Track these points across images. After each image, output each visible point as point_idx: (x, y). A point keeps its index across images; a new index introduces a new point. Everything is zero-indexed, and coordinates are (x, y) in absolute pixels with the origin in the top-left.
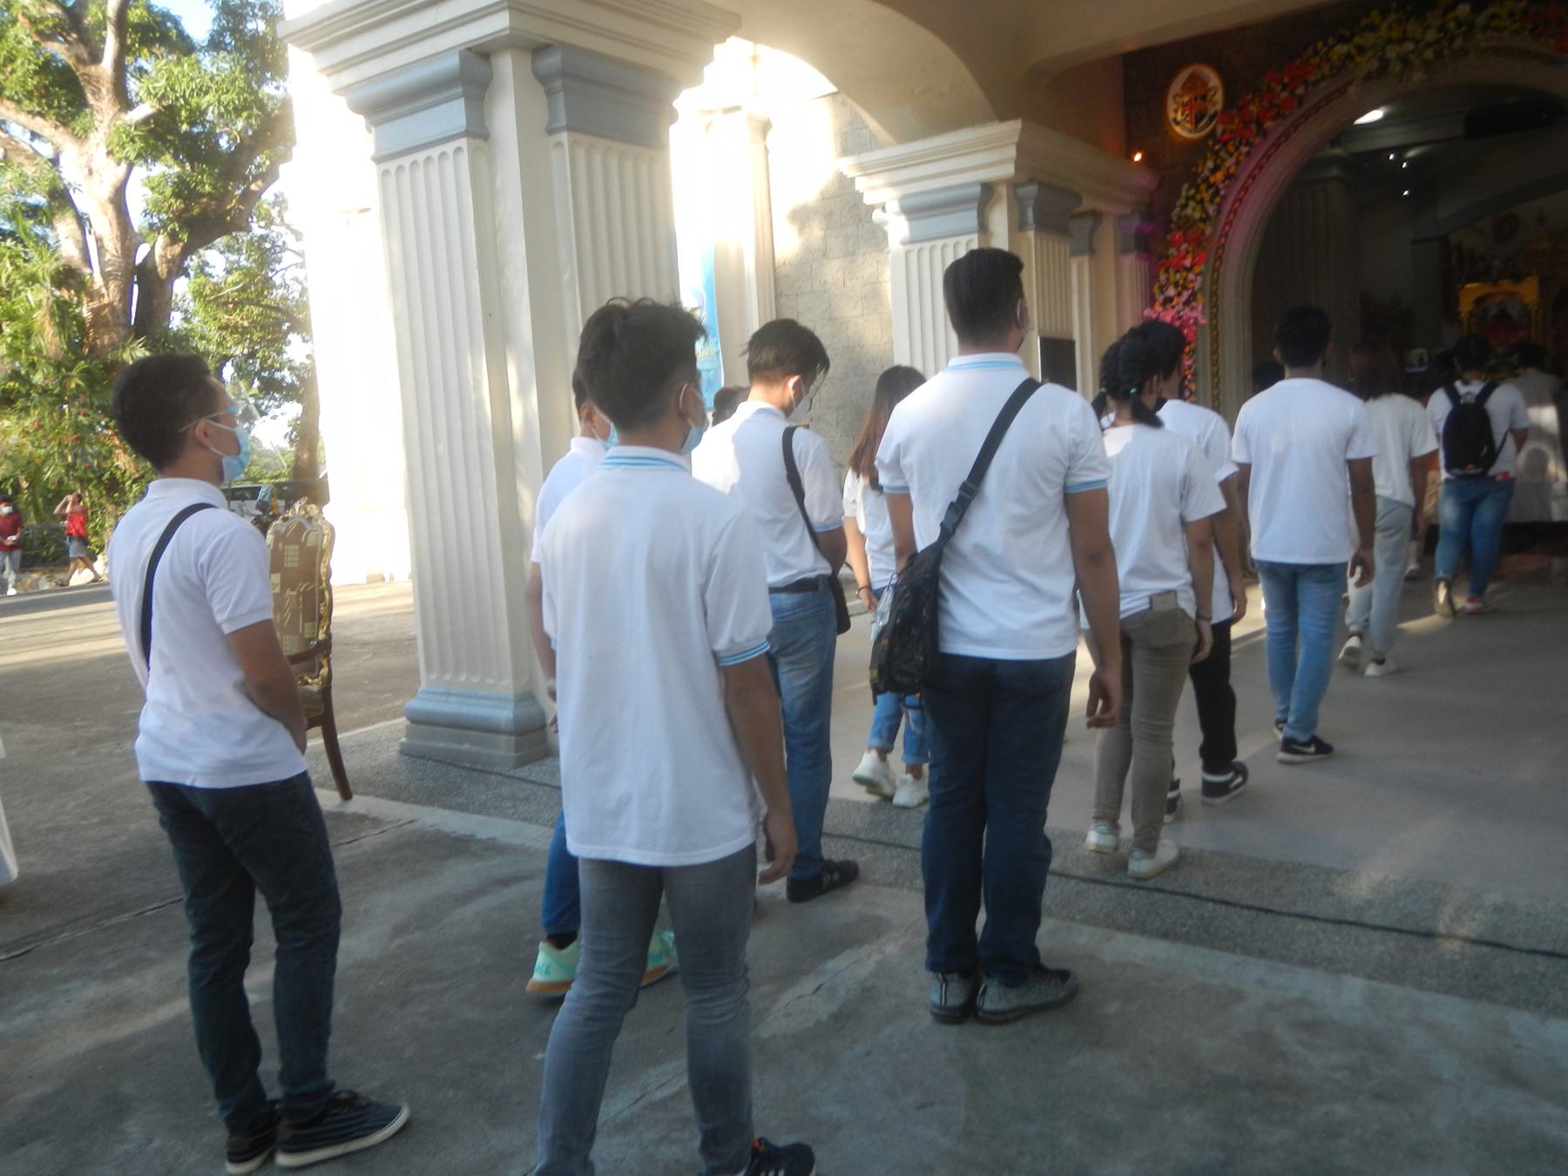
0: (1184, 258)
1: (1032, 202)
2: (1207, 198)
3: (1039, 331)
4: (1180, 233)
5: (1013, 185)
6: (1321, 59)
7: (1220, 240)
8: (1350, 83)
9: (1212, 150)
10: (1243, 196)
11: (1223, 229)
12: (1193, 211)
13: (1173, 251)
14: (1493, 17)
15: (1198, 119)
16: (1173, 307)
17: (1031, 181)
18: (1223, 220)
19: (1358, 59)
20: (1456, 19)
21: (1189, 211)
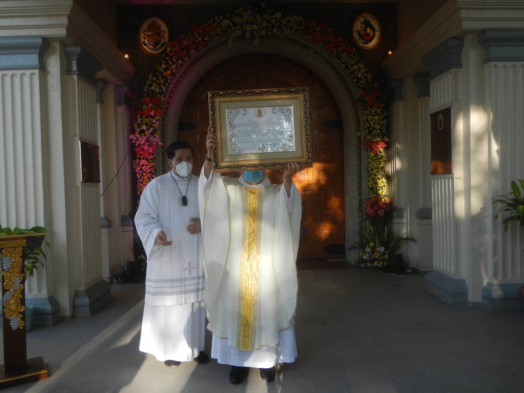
0: (151, 111)
1: (76, 57)
2: (162, 83)
3: (80, 138)
4: (149, 98)
5: (64, 43)
6: (217, 26)
8: (229, 40)
11: (167, 101)
13: (144, 107)
15: (156, 44)
16: (145, 135)
17: (75, 44)
18: (168, 96)
19: (233, 28)
20: (276, 18)
21: (153, 88)
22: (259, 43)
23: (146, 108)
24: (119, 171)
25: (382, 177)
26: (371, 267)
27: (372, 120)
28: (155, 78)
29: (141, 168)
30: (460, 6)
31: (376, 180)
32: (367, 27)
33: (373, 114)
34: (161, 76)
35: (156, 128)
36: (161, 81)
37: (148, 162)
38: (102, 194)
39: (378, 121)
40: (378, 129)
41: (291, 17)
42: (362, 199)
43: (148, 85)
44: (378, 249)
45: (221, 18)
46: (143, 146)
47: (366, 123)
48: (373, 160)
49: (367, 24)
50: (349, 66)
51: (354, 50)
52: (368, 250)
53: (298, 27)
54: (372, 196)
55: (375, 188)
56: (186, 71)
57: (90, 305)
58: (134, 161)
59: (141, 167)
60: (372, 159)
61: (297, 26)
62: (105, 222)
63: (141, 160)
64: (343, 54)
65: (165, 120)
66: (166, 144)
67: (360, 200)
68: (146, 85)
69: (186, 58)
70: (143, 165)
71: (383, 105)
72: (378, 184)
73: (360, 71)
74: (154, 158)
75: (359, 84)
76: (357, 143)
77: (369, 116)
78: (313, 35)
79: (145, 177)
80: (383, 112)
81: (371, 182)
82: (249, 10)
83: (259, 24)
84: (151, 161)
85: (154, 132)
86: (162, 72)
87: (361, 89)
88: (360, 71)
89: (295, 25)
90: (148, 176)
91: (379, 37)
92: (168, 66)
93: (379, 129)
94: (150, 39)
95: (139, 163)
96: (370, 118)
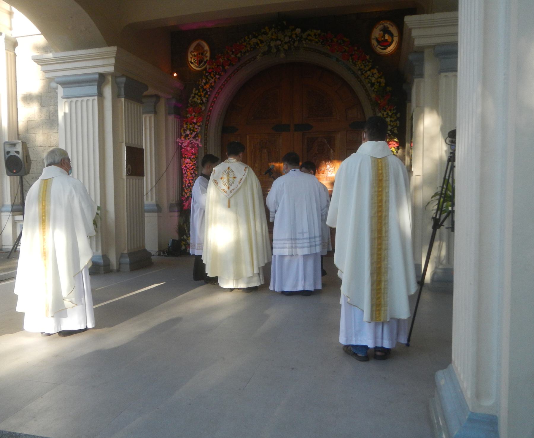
2: (203, 95)
4: (192, 108)
6: (247, 44)
7: (208, 113)
8: (257, 55)
9: (205, 75)
10: (217, 96)
11: (210, 109)
12: (197, 100)
13: (189, 115)
14: (309, 35)
15: (200, 62)
16: (189, 139)
18: (209, 105)
19: (260, 45)
20: (296, 34)
21: (195, 99)
28: (197, 92)
29: (186, 165)
35: (198, 132)
36: (202, 93)
37: (191, 160)
39: (390, 122)
41: (310, 32)
43: (192, 97)
45: (250, 37)
46: (187, 147)
51: (368, 57)
58: (182, 160)
59: (185, 164)
61: (316, 38)
62: (156, 208)
65: (207, 125)
69: (223, 72)
70: (187, 163)
71: (395, 108)
74: (196, 157)
75: (373, 88)
78: (331, 46)
82: (273, 29)
84: (193, 160)
85: (196, 136)
86: (203, 86)
91: (397, 43)
92: (207, 80)
94: (196, 58)
95: (184, 161)
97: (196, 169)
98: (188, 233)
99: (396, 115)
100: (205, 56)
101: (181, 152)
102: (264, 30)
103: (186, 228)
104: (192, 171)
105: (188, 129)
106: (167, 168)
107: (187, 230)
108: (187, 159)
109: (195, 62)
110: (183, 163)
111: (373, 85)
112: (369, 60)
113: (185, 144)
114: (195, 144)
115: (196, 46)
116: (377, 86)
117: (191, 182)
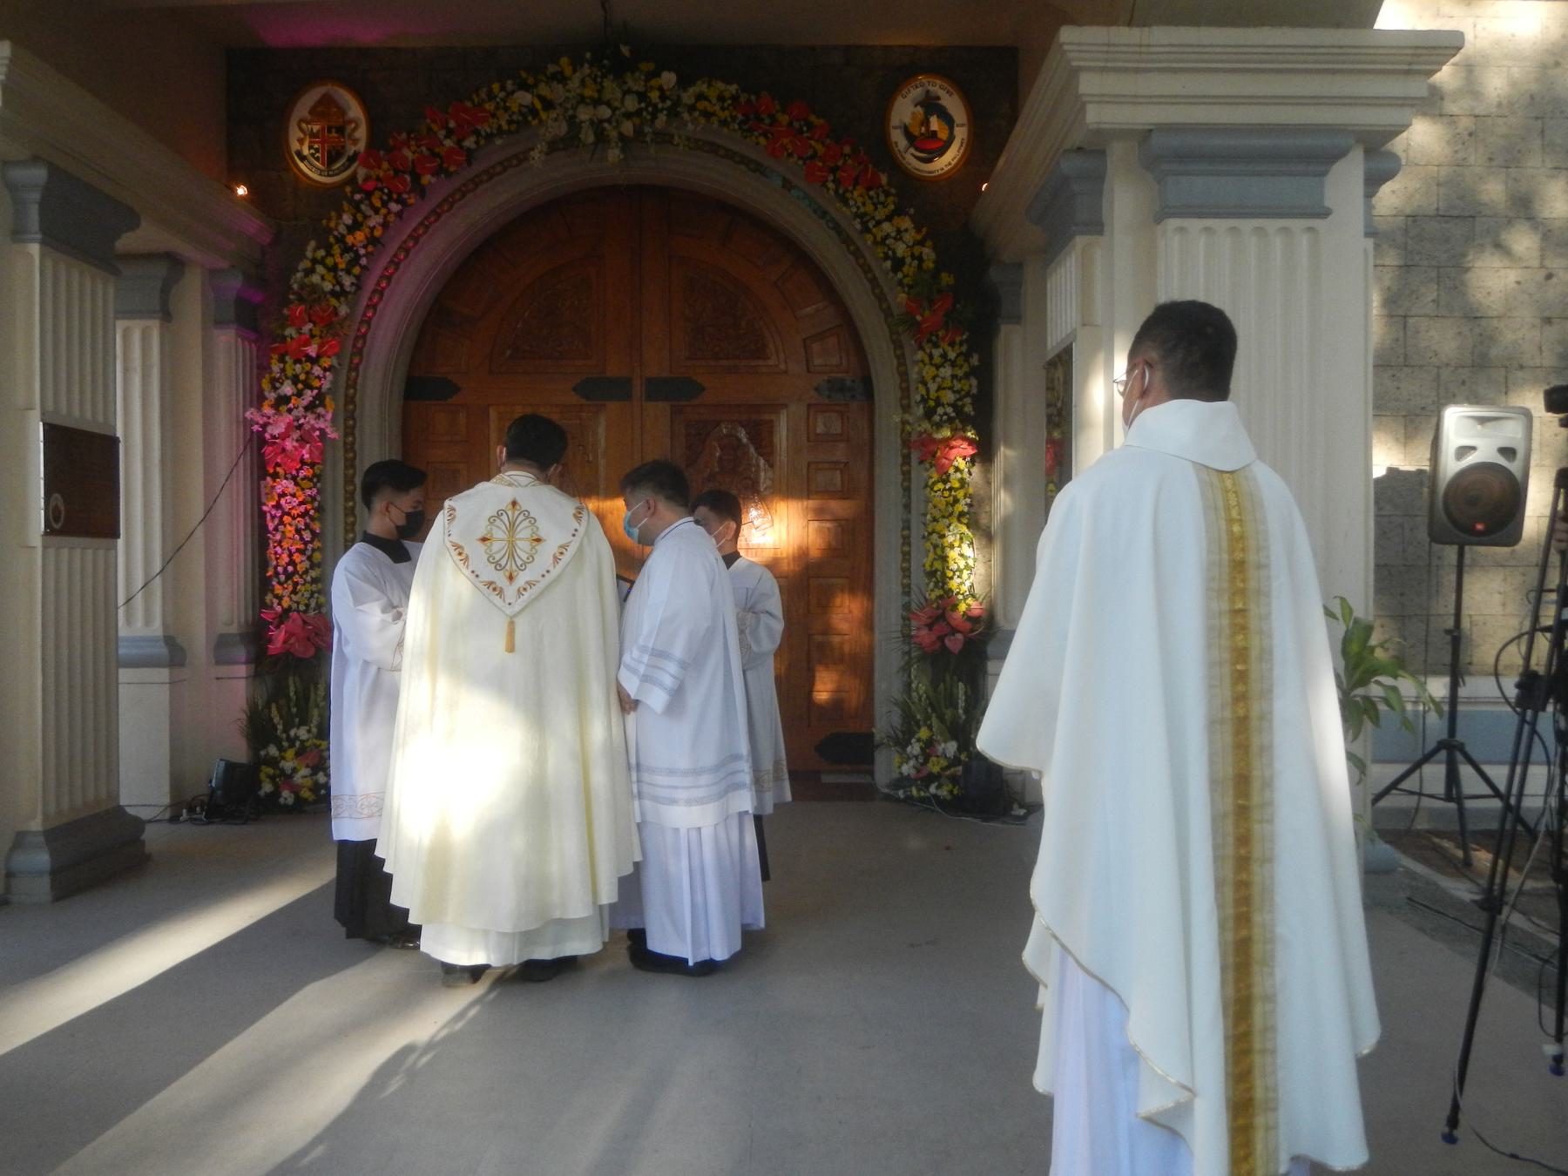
0: (307, 343)
1: (36, 196)
2: (342, 266)
3: (43, 413)
4: (303, 306)
6: (497, 108)
7: (359, 330)
12: (321, 279)
13: (290, 331)
15: (332, 158)
16: (290, 411)
17: (36, 159)
18: (364, 302)
19: (543, 115)
20: (661, 89)
21: (315, 279)
22: (619, 156)
23: (294, 336)
24: (211, 508)
25: (961, 539)
26: (923, 800)
27: (934, 378)
28: (321, 253)
29: (278, 502)
30: (1074, 64)
31: (943, 548)
32: (932, 115)
33: (937, 360)
34: (340, 247)
35: (323, 390)
36: (338, 260)
37: (296, 484)
38: (158, 571)
39: (952, 382)
40: (949, 405)
41: (705, 86)
42: (909, 602)
44: (940, 748)
45: (509, 85)
46: (283, 439)
47: (920, 386)
48: (936, 492)
49: (931, 105)
50: (871, 225)
51: (884, 179)
52: (915, 748)
53: (727, 113)
54: (933, 596)
55: (939, 573)
56: (421, 232)
57: (55, 873)
58: (262, 483)
59: (276, 498)
60: (935, 489)
61: (723, 109)
62: (162, 650)
63: (278, 480)
64: (854, 188)
65: (356, 369)
66: (357, 435)
67: (907, 607)
68: (298, 271)
71: (964, 337)
72: (948, 562)
73: (901, 239)
74: (314, 475)
75: (900, 275)
76: (899, 441)
77: (927, 367)
78: (769, 135)
79: (288, 527)
80: (967, 356)
81: (931, 555)
82: (586, 65)
83: (616, 104)
84: (305, 484)
86: (343, 236)
87: (906, 289)
88: (901, 239)
89: (717, 108)
90: (296, 526)
91: (965, 141)
93: (954, 405)
95: (273, 487)
96: (933, 371)
97: (317, 515)
98: (284, 736)
99: (967, 360)
100: (350, 136)
101: (261, 456)
102: (557, 69)
103: (276, 720)
104: (301, 523)
105: (287, 378)
106: (208, 511)
107: (280, 727)
108: (285, 481)
109: (313, 155)
110: (267, 494)
111: (898, 264)
112: (886, 188)
113: (277, 429)
114: (314, 429)
115: (320, 102)
116: (910, 268)
117: (297, 561)
